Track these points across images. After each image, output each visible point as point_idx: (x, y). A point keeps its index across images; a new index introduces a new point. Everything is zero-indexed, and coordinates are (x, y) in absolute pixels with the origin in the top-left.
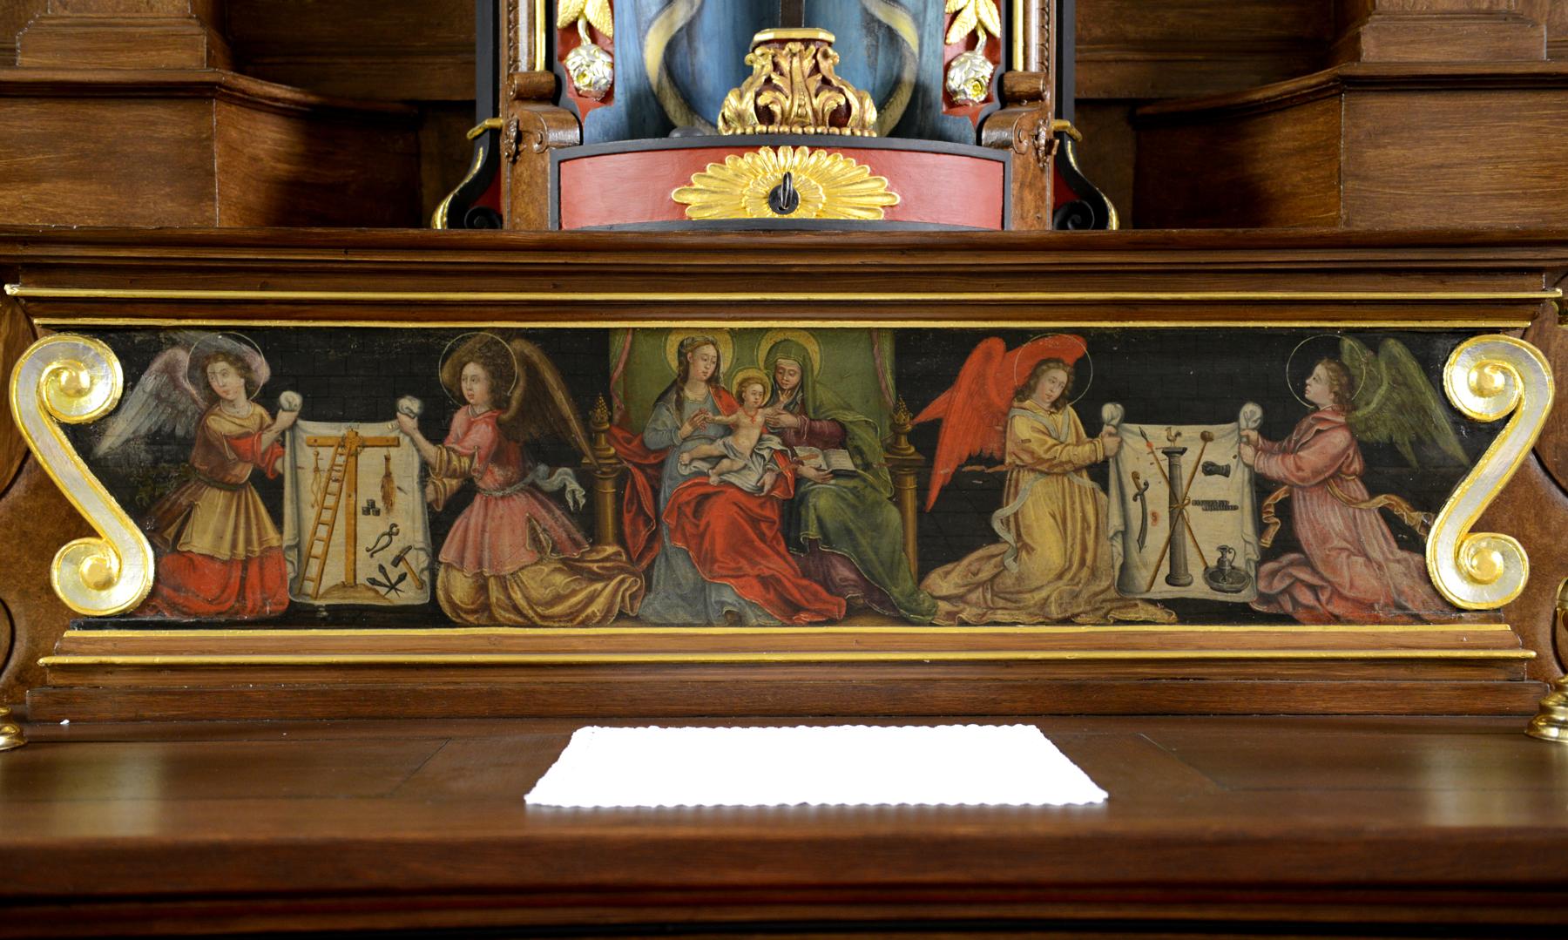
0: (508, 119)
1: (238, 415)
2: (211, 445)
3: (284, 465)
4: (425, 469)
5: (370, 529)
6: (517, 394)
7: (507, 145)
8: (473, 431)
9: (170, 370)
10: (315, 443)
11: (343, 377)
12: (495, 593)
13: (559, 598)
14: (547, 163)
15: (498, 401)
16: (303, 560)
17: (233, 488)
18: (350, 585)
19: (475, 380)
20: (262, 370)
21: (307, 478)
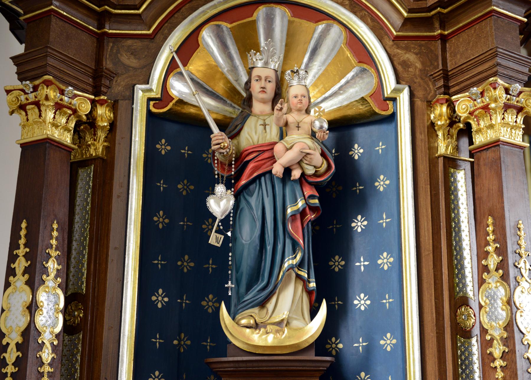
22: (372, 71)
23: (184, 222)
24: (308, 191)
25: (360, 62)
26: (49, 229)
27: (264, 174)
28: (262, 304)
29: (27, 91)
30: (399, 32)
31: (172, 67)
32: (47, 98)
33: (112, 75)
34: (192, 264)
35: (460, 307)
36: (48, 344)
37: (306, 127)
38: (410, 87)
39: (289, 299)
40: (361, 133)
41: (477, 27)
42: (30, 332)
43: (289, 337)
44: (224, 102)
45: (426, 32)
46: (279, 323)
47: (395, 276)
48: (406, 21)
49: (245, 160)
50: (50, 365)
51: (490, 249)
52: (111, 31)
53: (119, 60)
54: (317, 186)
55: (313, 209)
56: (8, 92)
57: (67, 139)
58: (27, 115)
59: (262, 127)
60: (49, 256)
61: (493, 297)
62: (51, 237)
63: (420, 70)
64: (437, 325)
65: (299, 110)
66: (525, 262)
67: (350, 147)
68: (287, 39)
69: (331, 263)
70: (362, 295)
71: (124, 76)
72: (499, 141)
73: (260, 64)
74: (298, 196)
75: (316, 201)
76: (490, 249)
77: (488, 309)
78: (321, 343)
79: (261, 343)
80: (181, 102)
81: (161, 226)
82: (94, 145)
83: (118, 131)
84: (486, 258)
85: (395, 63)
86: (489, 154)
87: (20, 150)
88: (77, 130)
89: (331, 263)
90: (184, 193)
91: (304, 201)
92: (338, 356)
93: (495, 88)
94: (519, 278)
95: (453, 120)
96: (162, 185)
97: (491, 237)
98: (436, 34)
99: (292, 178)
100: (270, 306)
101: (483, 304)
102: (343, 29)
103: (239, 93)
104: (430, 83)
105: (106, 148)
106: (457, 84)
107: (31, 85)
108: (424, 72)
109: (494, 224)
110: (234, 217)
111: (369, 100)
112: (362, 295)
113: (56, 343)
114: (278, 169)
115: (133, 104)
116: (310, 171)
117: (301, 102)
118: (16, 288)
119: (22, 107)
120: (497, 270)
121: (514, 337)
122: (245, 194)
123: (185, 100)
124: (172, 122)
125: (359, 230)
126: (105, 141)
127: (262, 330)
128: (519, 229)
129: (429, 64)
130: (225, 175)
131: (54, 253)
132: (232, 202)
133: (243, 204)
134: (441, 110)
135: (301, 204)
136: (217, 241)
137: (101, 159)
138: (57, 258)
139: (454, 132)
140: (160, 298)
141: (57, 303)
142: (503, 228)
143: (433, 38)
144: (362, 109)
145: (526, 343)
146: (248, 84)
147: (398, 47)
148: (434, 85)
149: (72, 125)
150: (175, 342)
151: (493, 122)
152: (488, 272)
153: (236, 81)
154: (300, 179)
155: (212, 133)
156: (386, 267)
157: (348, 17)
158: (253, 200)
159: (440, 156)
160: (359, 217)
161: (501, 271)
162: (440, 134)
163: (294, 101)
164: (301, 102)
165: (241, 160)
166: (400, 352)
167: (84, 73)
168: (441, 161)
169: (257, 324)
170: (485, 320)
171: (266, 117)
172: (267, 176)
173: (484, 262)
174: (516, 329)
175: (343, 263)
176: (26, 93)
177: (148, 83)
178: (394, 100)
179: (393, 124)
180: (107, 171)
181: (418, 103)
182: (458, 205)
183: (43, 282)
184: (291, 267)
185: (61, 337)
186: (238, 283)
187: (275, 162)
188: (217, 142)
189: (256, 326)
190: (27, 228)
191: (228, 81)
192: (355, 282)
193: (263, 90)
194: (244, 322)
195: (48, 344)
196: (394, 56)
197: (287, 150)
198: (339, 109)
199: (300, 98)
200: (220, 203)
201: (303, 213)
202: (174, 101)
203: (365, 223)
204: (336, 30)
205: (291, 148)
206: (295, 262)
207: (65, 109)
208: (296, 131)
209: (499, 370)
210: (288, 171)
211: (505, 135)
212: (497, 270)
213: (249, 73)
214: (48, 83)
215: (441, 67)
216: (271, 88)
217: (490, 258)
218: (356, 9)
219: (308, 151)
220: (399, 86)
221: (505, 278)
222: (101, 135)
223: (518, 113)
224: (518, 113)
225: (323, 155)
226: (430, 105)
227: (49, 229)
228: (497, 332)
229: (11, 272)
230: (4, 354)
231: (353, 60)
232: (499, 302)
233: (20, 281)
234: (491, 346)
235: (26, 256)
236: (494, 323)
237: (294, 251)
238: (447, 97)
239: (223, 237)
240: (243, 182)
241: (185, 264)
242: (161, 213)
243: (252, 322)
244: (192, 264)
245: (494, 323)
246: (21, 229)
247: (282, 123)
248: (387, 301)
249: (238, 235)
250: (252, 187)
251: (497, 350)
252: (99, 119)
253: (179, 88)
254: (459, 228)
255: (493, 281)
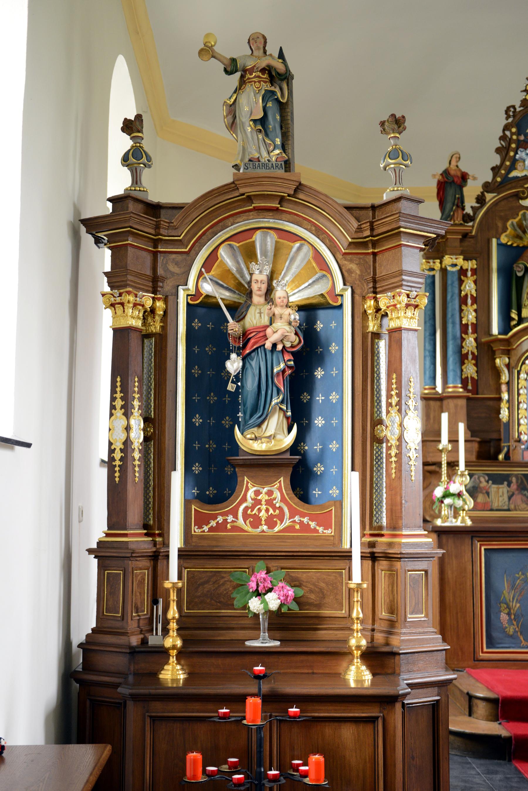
0: (512, 443)
1: (484, 484)
2: (480, 488)
3: (490, 491)
4: (508, 491)
5: (501, 499)
6: (519, 481)
7: (511, 448)
8: (514, 486)
9: (475, 478)
10: (494, 488)
11: (497, 479)
12: (517, 507)
13: (525, 508)
14: (521, 451)
15: (517, 482)
16: (492, 503)
17: (483, 493)
18: (498, 506)
19: (514, 480)
20: (487, 478)
21: (493, 492)
22: (329, 276)
23: (210, 371)
24: (287, 357)
25: (321, 270)
26: (133, 381)
27: (260, 347)
28: (259, 426)
29: (115, 296)
30: (346, 249)
31: (200, 274)
32: (129, 302)
33: (163, 279)
34: (216, 398)
35: (377, 425)
36: (137, 449)
37: (285, 317)
38: (352, 287)
39: (275, 423)
40: (322, 314)
41: (393, 251)
42: (127, 443)
43: (275, 445)
44: (235, 292)
45: (363, 250)
46: (269, 437)
47: (339, 406)
48: (350, 244)
49: (249, 337)
50: (139, 460)
51: (393, 393)
52: (162, 250)
53: (168, 269)
54: (293, 353)
55: (290, 367)
56: (103, 295)
57: (138, 324)
58: (115, 309)
59: (259, 315)
60: (134, 398)
61: (393, 422)
62: (134, 386)
63: (359, 275)
64: (362, 437)
65: (282, 306)
66: (412, 401)
67: (315, 323)
68: (275, 252)
69: (302, 397)
70: (320, 418)
71: (171, 279)
72: (401, 328)
73: (257, 272)
74: (281, 361)
75: (292, 363)
76: (393, 393)
77: (390, 428)
78: (294, 449)
79: (259, 449)
80: (207, 296)
81: (196, 376)
82: (154, 325)
83: (168, 316)
84: (391, 398)
85: (343, 271)
86: (396, 335)
87: (112, 332)
88: (144, 318)
89: (302, 397)
90: (210, 353)
91: (284, 364)
92: (304, 455)
93: (400, 296)
94: (408, 411)
95: (378, 310)
96: (196, 349)
97: (394, 386)
98: (369, 251)
99: (277, 350)
100: (264, 426)
101: (388, 425)
102: (311, 247)
103: (244, 286)
104: (365, 284)
105: (162, 327)
106: (381, 287)
107: (118, 293)
108: (361, 276)
109: (396, 378)
110: (242, 374)
111: (326, 295)
112: (320, 418)
113: (140, 448)
114: (268, 345)
115: (178, 299)
116: (288, 345)
117: (283, 301)
118: (116, 417)
119: (113, 305)
120: (396, 406)
121: (401, 445)
122: (250, 361)
123: (210, 295)
124: (203, 309)
125: (319, 377)
126: (161, 322)
127: (259, 441)
128: (410, 382)
129: (365, 271)
130: (237, 346)
131: (137, 396)
132: (241, 364)
133: (247, 365)
134: (371, 303)
135: (282, 365)
136: (232, 388)
137: (160, 334)
138: (139, 398)
139: (379, 316)
140: (197, 420)
141: (139, 425)
142: (401, 381)
143: (368, 254)
144: (322, 300)
145: (408, 448)
146: (249, 283)
147: (346, 260)
148: (367, 286)
149: (141, 315)
150: (207, 446)
151: (399, 315)
152: (392, 407)
153: (242, 277)
154: (282, 350)
155: (228, 322)
156: (334, 401)
157: (314, 240)
158: (254, 363)
159: (369, 332)
160: (319, 369)
161: (398, 407)
162: (370, 317)
163: (278, 301)
164: (283, 301)
165: (245, 336)
166: (340, 452)
167: (148, 280)
168: (370, 335)
169: (256, 437)
170: (389, 435)
171: (261, 307)
172: (262, 348)
173: (390, 401)
174: (403, 440)
175: (309, 397)
176: (114, 297)
177: (186, 285)
178: (342, 296)
179: (342, 310)
180: (162, 341)
181: (357, 297)
182: (379, 363)
183: (132, 413)
184: (277, 404)
185: (143, 445)
186: (245, 413)
187: (267, 339)
188: (231, 328)
189: (256, 439)
190: (120, 381)
191: (235, 278)
192: (316, 409)
193: (259, 289)
194: (249, 436)
195: (137, 449)
196: (343, 265)
197: (274, 332)
198: (308, 299)
199: (282, 299)
200: (234, 364)
201: (284, 371)
202: (203, 296)
203: (323, 373)
204: (306, 248)
205: (276, 331)
206: (279, 401)
207: (138, 306)
208: (279, 320)
209: (393, 463)
210: (274, 345)
211: (405, 324)
212: (396, 406)
213: (251, 275)
214: (129, 293)
215: (372, 275)
216: (264, 287)
217: (393, 399)
218: (319, 233)
219: (287, 334)
220: (345, 287)
221: (400, 411)
222: (158, 318)
223: (415, 309)
224: (415, 309)
225: (296, 334)
226: (364, 298)
227: (133, 381)
228: (394, 442)
229: (113, 407)
230: (113, 454)
231: (317, 269)
232: (396, 424)
233: (119, 413)
234: (390, 450)
235: (122, 398)
236: (392, 437)
237: (278, 394)
238: (374, 295)
239: (235, 386)
240: (248, 352)
241: (212, 398)
242: (196, 367)
243: (253, 436)
244: (216, 398)
245: (392, 437)
246: (117, 382)
247: (271, 315)
248: (334, 422)
249: (245, 385)
250: (253, 354)
251: (393, 452)
252: (157, 309)
253: (207, 288)
254: (379, 378)
255: (394, 411)
